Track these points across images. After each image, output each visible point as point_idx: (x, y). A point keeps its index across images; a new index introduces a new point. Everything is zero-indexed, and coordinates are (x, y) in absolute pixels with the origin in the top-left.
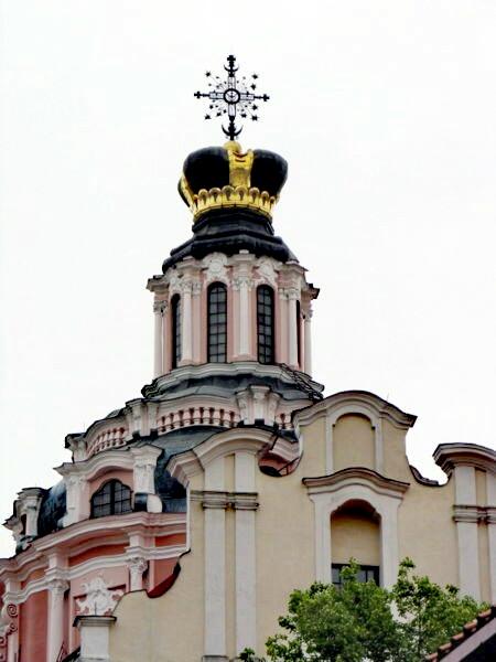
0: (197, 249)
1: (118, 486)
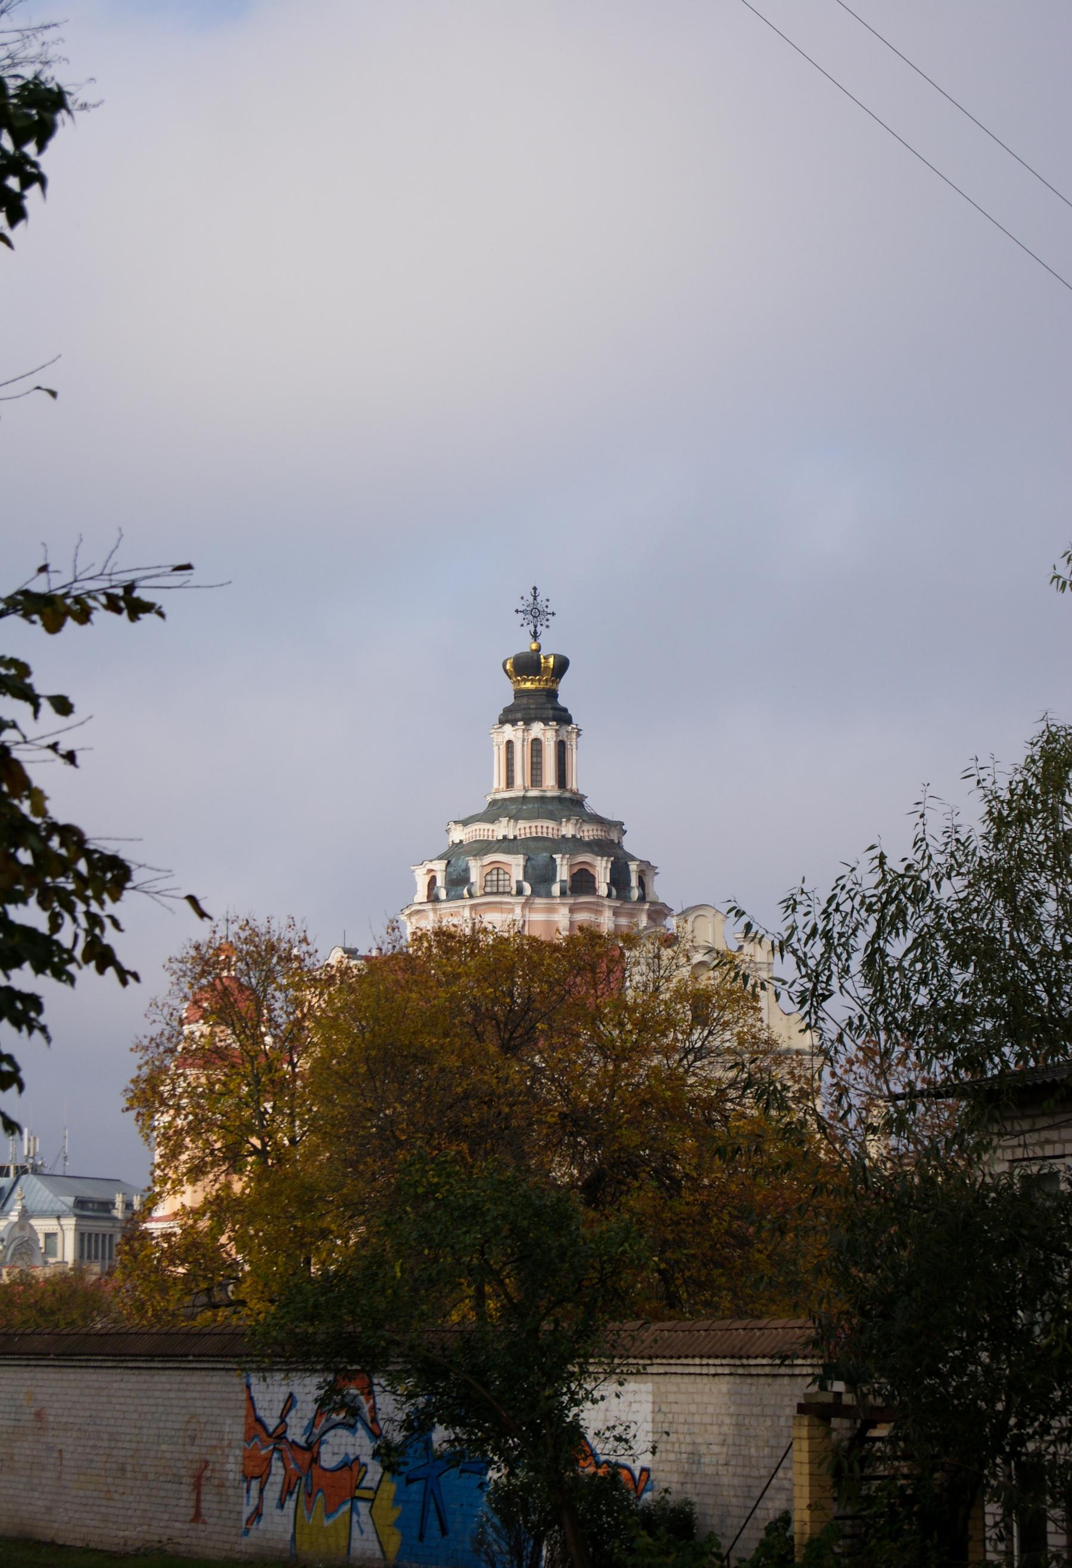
1: (501, 872)
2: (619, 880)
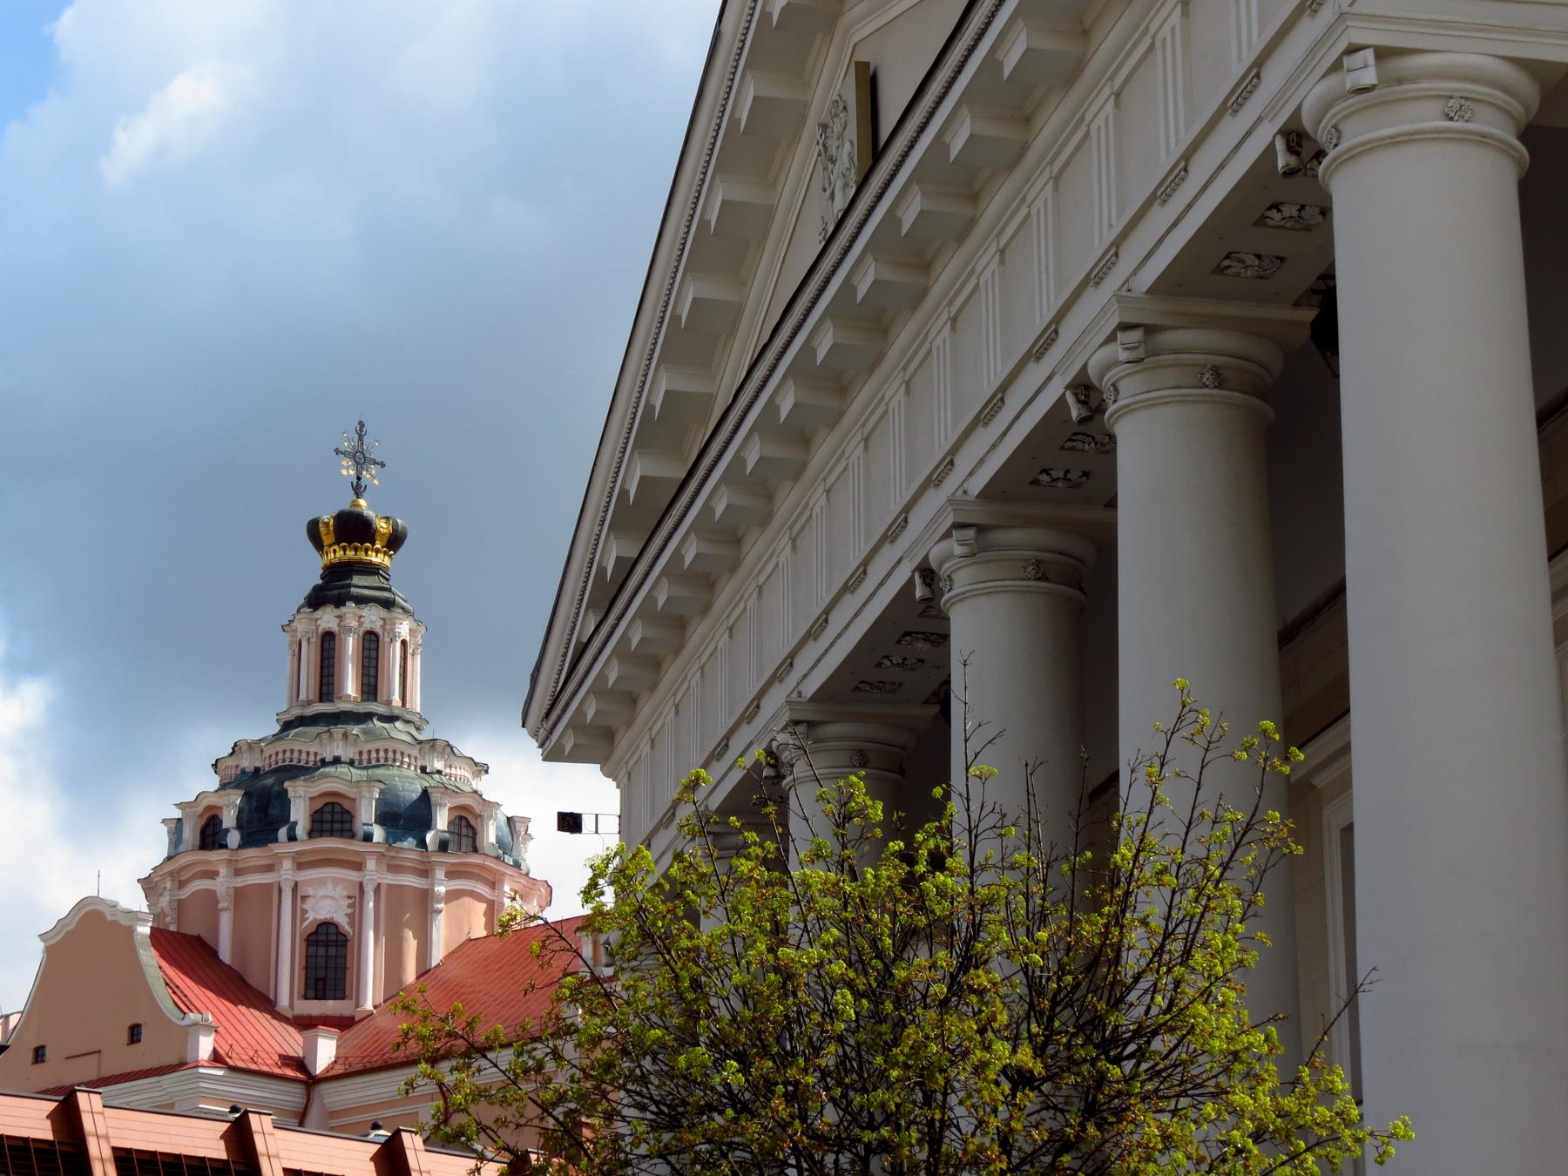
0: (316, 600)
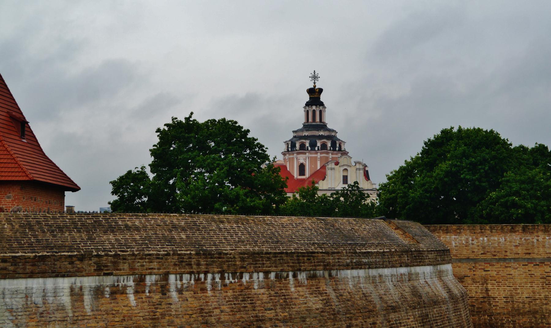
2: (334, 145)
